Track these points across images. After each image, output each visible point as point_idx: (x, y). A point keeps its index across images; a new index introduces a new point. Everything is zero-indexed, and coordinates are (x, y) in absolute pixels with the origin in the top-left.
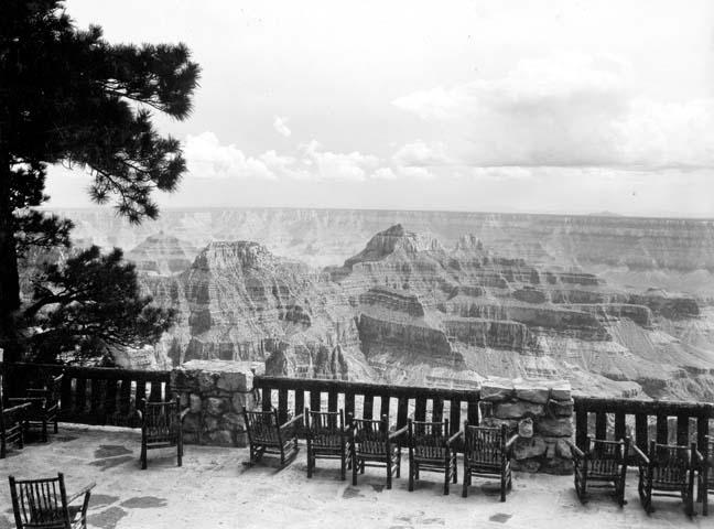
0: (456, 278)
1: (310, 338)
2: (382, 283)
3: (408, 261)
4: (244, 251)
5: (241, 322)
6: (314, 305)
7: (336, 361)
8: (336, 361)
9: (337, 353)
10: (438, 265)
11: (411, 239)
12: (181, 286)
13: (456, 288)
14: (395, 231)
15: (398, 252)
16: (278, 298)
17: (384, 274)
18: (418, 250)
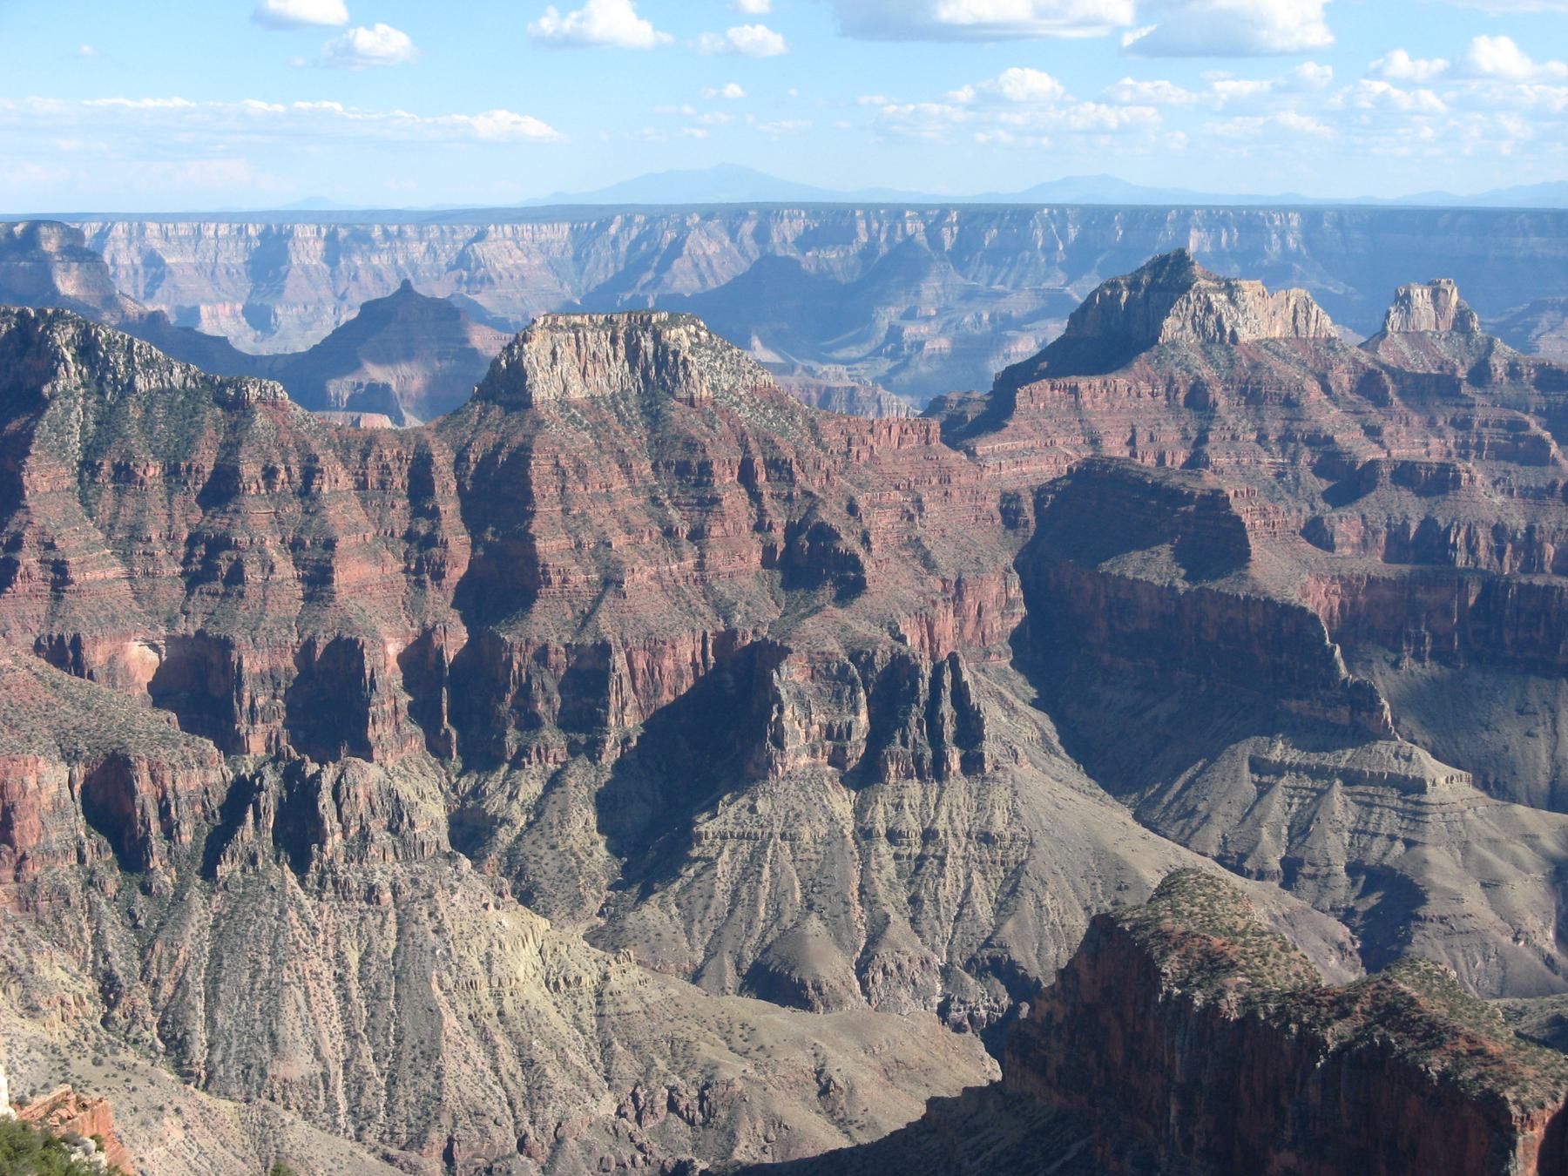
0: (1373, 432)
1: (863, 628)
2: (1115, 447)
3: (1207, 373)
4: (647, 344)
5: (639, 577)
6: (883, 523)
7: (947, 708)
8: (947, 708)
9: (947, 679)
10: (1313, 388)
11: (1219, 300)
12: (442, 459)
13: (1373, 464)
14: (1170, 276)
15: (1174, 344)
16: (755, 496)
17: (1122, 417)
18: (1245, 335)
